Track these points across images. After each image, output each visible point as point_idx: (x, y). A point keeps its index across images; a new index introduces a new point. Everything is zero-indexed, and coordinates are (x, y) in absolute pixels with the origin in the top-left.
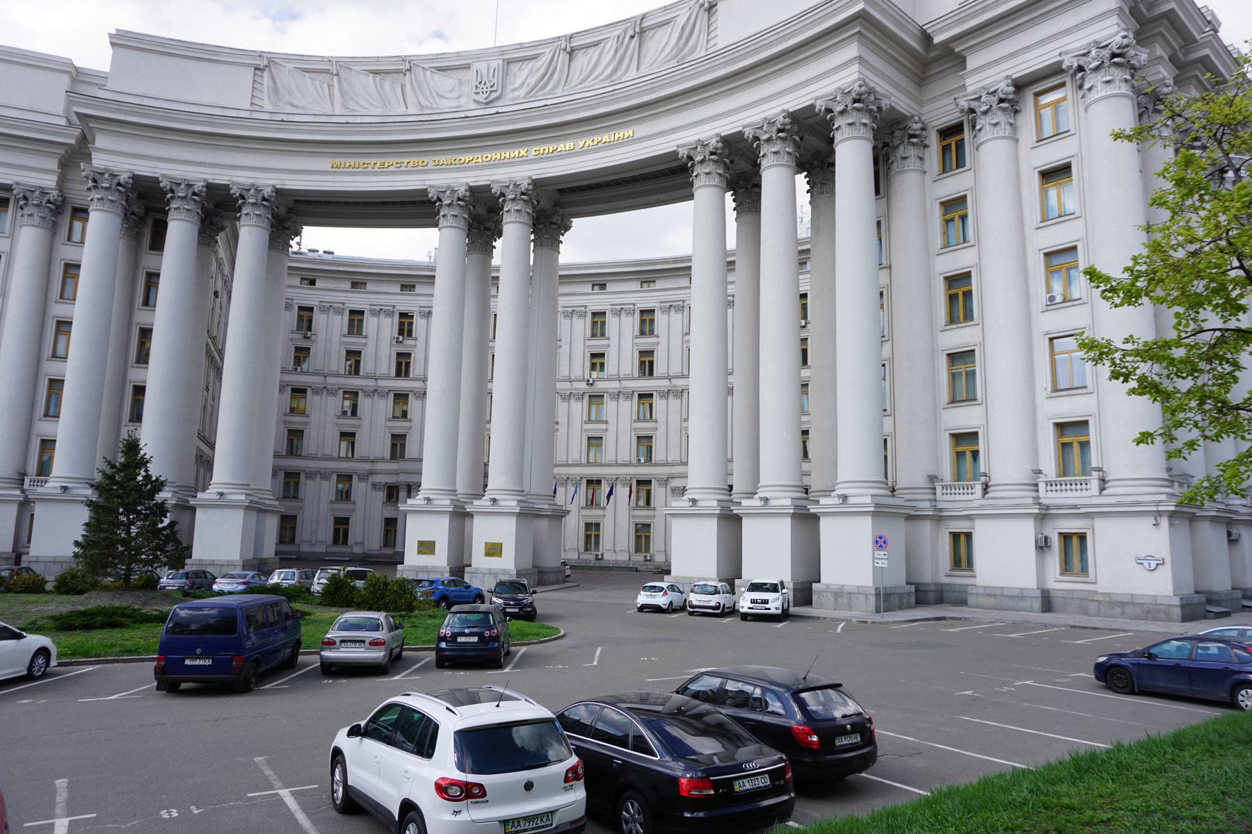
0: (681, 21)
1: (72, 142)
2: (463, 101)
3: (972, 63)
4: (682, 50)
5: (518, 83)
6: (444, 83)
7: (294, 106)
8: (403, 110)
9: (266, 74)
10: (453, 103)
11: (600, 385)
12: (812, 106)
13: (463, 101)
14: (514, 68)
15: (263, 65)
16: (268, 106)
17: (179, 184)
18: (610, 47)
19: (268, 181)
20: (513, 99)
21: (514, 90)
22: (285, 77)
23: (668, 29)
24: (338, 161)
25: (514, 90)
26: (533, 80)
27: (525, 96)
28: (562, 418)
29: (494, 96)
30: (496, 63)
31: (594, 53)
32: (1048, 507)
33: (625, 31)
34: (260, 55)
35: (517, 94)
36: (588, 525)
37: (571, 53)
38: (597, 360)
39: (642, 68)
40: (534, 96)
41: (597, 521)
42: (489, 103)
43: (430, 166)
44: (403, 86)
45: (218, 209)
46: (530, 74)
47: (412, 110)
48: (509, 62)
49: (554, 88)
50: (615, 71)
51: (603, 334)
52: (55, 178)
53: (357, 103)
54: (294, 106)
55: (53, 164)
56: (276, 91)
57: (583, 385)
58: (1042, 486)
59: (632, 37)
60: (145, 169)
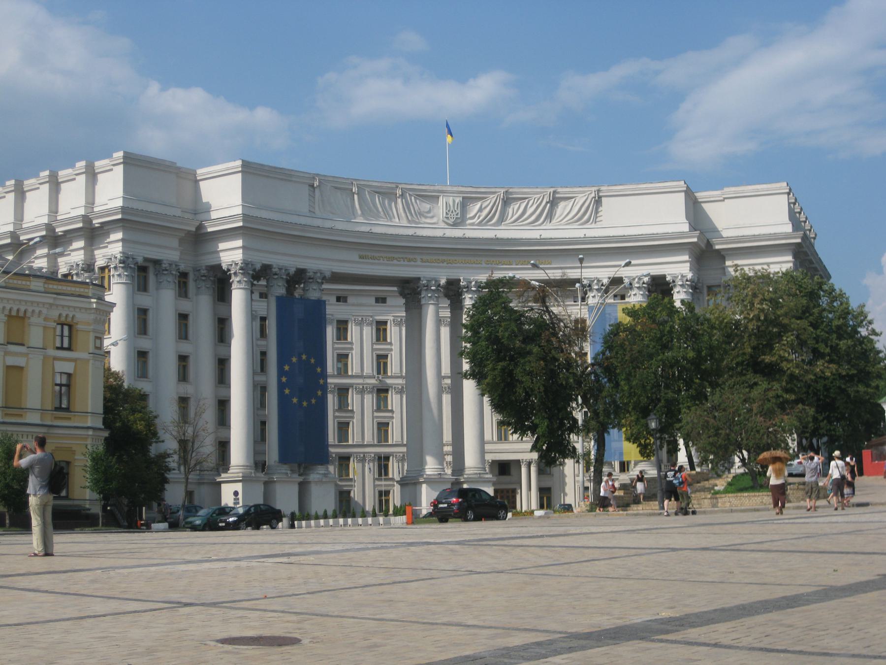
2: (434, 220)
5: (472, 215)
9: (317, 191)
12: (664, 277)
13: (434, 220)
27: (480, 224)
28: (356, 408)
30: (458, 200)
36: (380, 493)
39: (554, 221)
40: (486, 224)
41: (387, 488)
44: (396, 203)
46: (481, 210)
47: (405, 223)
51: (385, 339)
55: (175, 243)
59: (547, 203)
60: (268, 259)
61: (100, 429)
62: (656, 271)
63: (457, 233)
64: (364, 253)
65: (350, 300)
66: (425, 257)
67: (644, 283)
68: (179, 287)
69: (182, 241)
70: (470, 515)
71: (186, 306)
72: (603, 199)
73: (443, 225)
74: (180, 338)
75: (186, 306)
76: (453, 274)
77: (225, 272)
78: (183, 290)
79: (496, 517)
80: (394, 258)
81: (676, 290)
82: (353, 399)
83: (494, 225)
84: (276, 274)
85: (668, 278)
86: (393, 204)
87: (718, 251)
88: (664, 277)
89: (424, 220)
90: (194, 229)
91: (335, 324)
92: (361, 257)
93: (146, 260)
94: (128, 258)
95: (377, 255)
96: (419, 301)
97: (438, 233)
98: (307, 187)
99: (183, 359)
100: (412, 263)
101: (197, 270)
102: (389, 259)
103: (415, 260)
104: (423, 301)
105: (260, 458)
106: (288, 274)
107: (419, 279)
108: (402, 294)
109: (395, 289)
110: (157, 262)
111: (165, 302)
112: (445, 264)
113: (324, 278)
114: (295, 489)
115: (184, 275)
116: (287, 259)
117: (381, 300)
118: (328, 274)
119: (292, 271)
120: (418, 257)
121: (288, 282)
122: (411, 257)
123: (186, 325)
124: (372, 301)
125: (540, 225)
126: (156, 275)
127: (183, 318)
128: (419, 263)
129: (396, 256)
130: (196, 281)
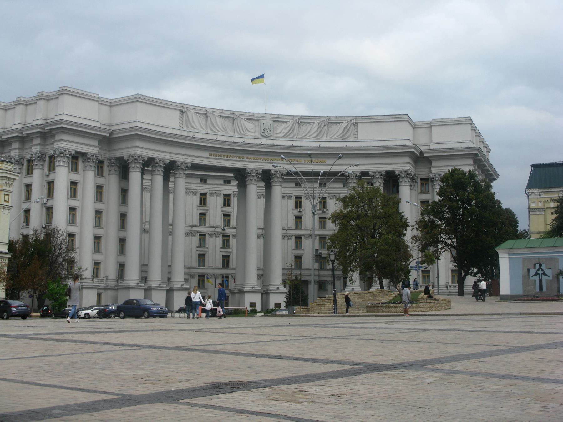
0: (344, 125)
1: (108, 135)
3: (434, 164)
4: (343, 136)
5: (278, 131)
6: (249, 125)
7: (193, 128)
8: (231, 134)
10: (253, 134)
11: (228, 230)
13: (257, 134)
14: (276, 124)
15: (183, 110)
16: (185, 129)
17: (160, 161)
18: (315, 127)
19: (189, 160)
20: (277, 137)
21: (277, 134)
22: (191, 115)
23: (339, 126)
24: (211, 153)
25: (277, 134)
26: (285, 131)
29: (270, 135)
30: (271, 122)
31: (309, 127)
32: (450, 292)
33: (322, 122)
34: (182, 105)
35: (278, 135)
37: (299, 124)
38: (227, 217)
39: (328, 137)
42: (267, 138)
43: (245, 159)
45: (170, 169)
47: (237, 135)
48: (274, 121)
49: (293, 136)
50: (317, 135)
52: (98, 149)
53: (216, 129)
54: (193, 128)
55: (96, 143)
56: (188, 121)
57: (219, 230)
58: (448, 287)
61: (5, 253)
62: (389, 168)
63: (270, 142)
64: (211, 153)
65: (209, 181)
66: (249, 156)
67: (381, 175)
68: (98, 169)
69: (100, 142)
70: (122, 314)
71: (101, 181)
72: (358, 124)
73: (260, 137)
74: (97, 200)
75: (101, 181)
76: (267, 166)
77: (126, 161)
78: (100, 172)
79: (137, 317)
80: (230, 156)
81: (401, 180)
82: (210, 241)
83: (292, 138)
84: (157, 163)
85: (397, 173)
86: (230, 124)
87: (426, 157)
88: (393, 172)
89: (248, 133)
90: (108, 135)
91: (198, 195)
92: (210, 155)
93: (77, 152)
94: (65, 151)
95: (220, 154)
96: (246, 182)
97: (258, 142)
98: (178, 112)
99: (98, 213)
100: (241, 159)
101: (109, 159)
102: (227, 157)
103: (243, 158)
104: (248, 183)
105: (144, 274)
106: (165, 164)
107: (245, 169)
108: (236, 178)
109: (232, 175)
110: (84, 154)
111: (88, 179)
112: (261, 161)
113: (187, 167)
114: (164, 294)
115: (100, 163)
116: (163, 154)
117: (227, 182)
118: (190, 165)
119: (167, 162)
120: (245, 156)
121: (165, 168)
122: (241, 156)
123: (101, 193)
124: (222, 182)
125: (319, 139)
126: (84, 162)
127: (99, 188)
128: (245, 159)
129: (232, 155)
130: (108, 166)
